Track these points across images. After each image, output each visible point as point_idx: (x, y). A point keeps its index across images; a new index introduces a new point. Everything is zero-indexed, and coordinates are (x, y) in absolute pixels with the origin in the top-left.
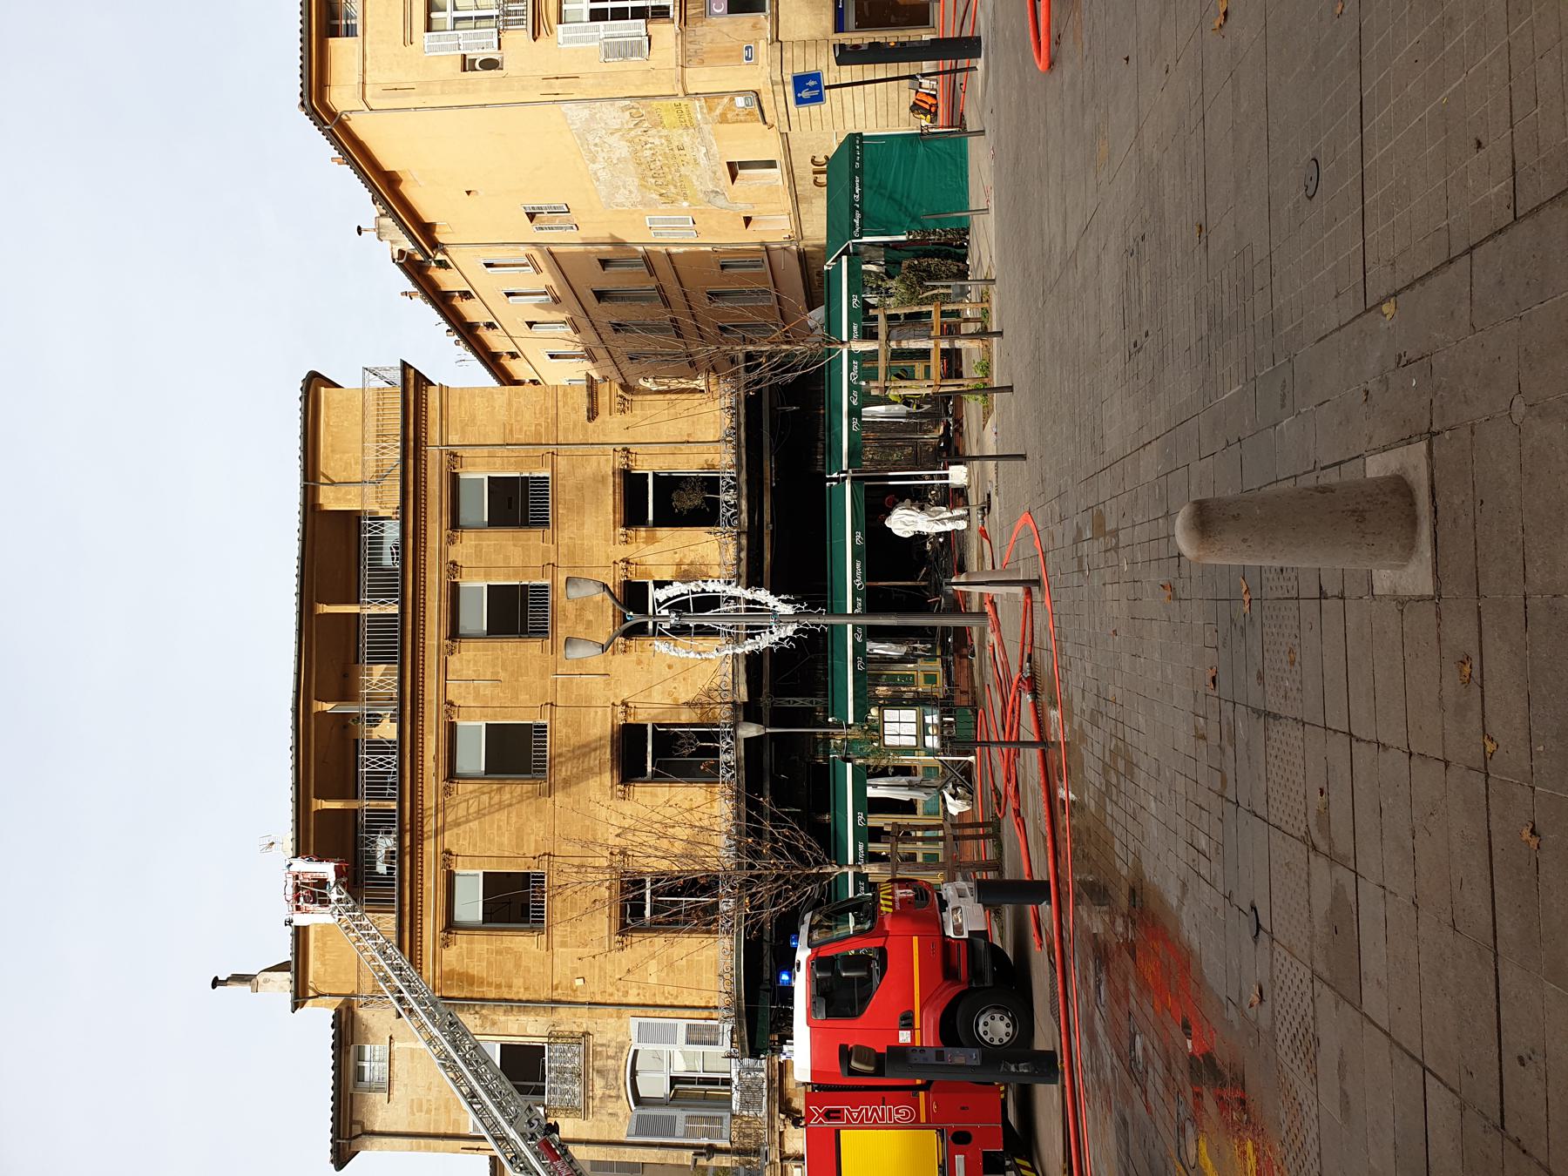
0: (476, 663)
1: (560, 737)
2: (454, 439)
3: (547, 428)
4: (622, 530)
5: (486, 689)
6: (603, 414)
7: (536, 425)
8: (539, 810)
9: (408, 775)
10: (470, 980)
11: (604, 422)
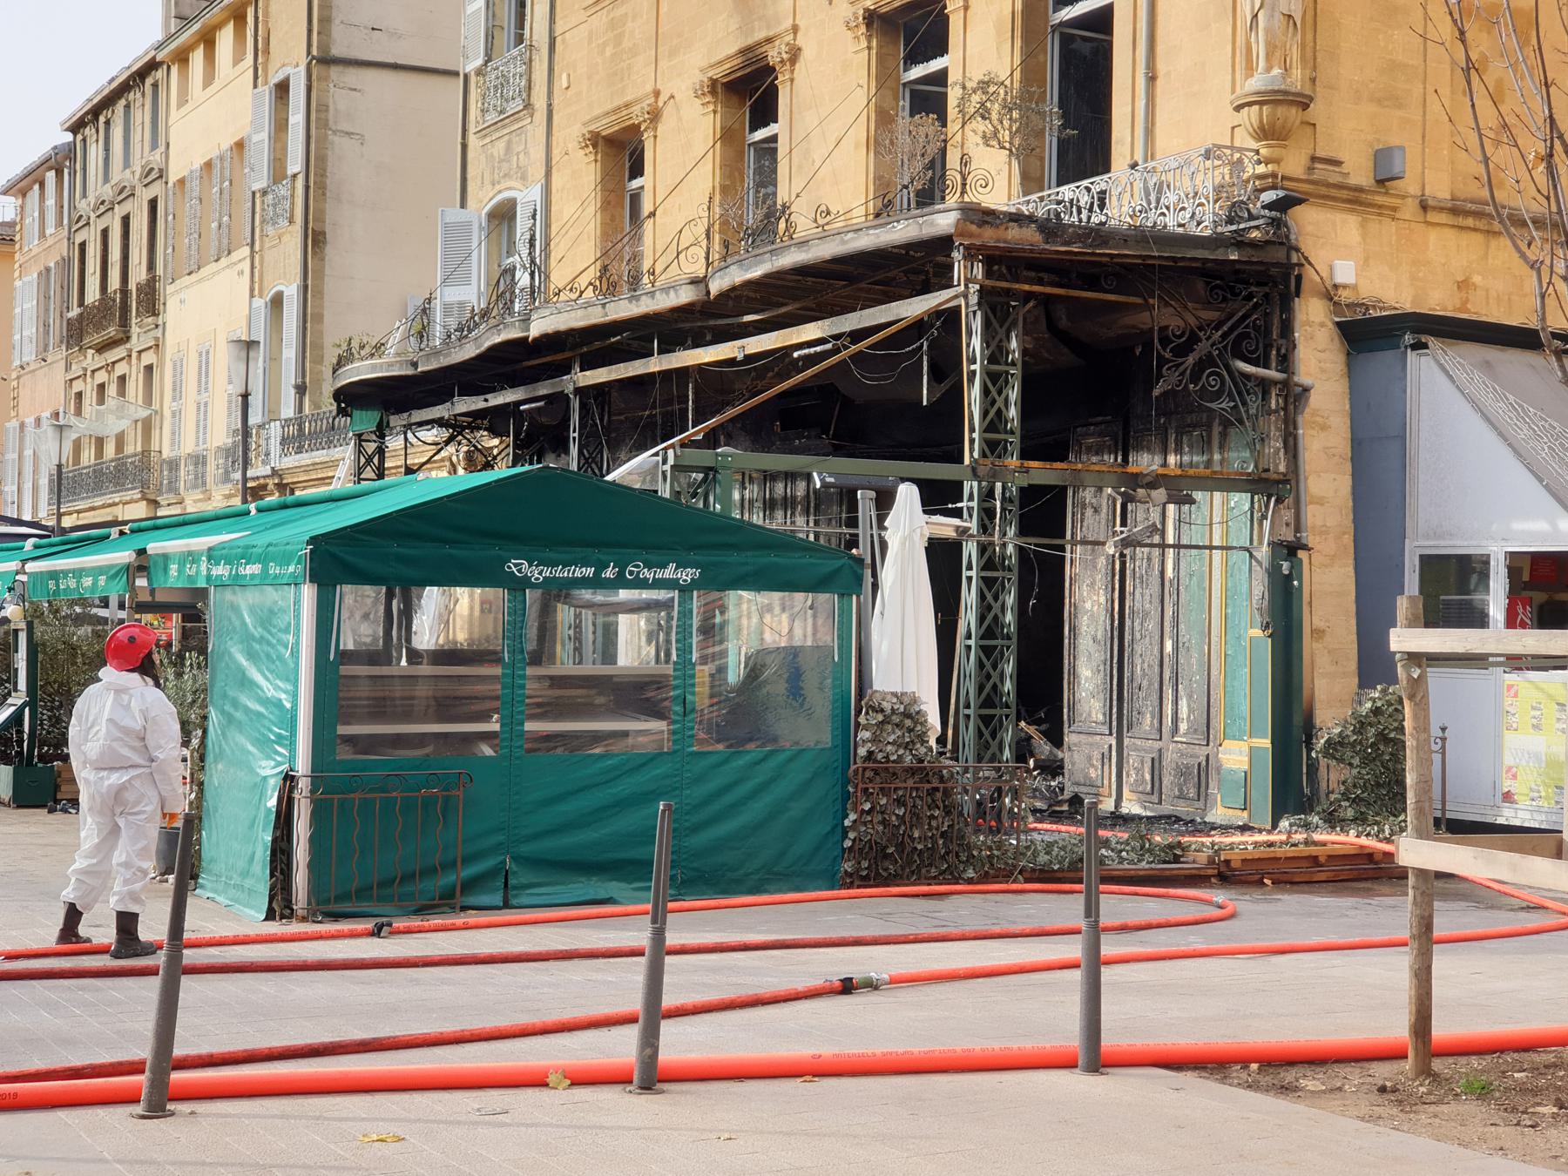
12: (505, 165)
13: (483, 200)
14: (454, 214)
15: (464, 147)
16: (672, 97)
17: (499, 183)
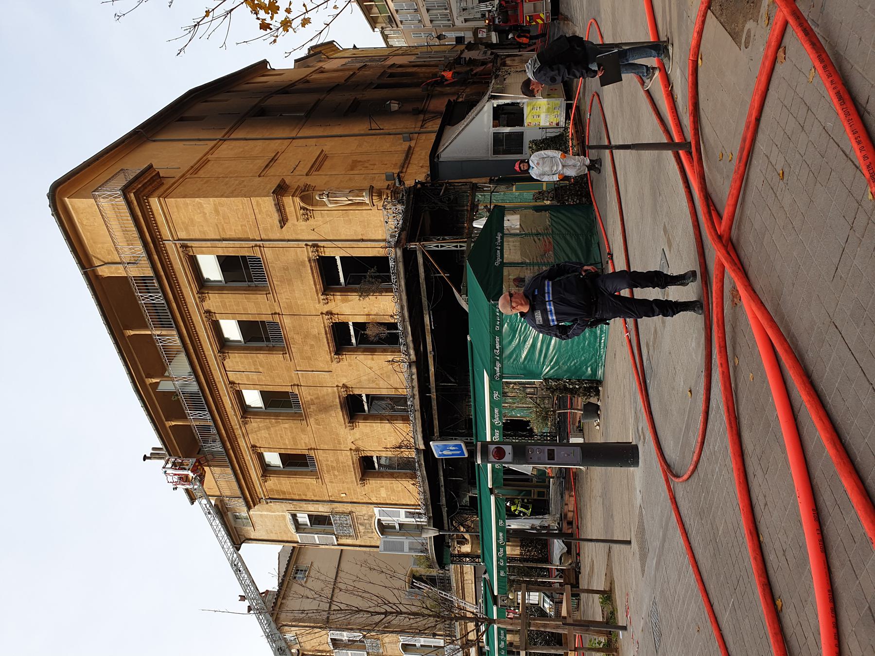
0: (242, 363)
1: (305, 395)
2: (182, 235)
3: (250, 228)
4: (322, 297)
5: (255, 376)
6: (292, 220)
7: (242, 226)
8: (303, 431)
9: (218, 419)
10: (284, 493)
11: (294, 225)
12: (368, 526)
13: (377, 538)
14: (382, 547)
15: (360, 546)
16: (352, 442)
17: (372, 529)
